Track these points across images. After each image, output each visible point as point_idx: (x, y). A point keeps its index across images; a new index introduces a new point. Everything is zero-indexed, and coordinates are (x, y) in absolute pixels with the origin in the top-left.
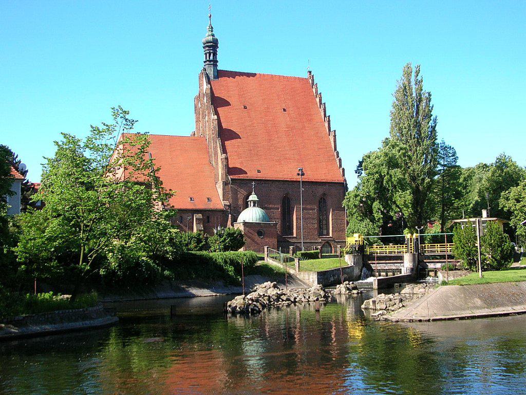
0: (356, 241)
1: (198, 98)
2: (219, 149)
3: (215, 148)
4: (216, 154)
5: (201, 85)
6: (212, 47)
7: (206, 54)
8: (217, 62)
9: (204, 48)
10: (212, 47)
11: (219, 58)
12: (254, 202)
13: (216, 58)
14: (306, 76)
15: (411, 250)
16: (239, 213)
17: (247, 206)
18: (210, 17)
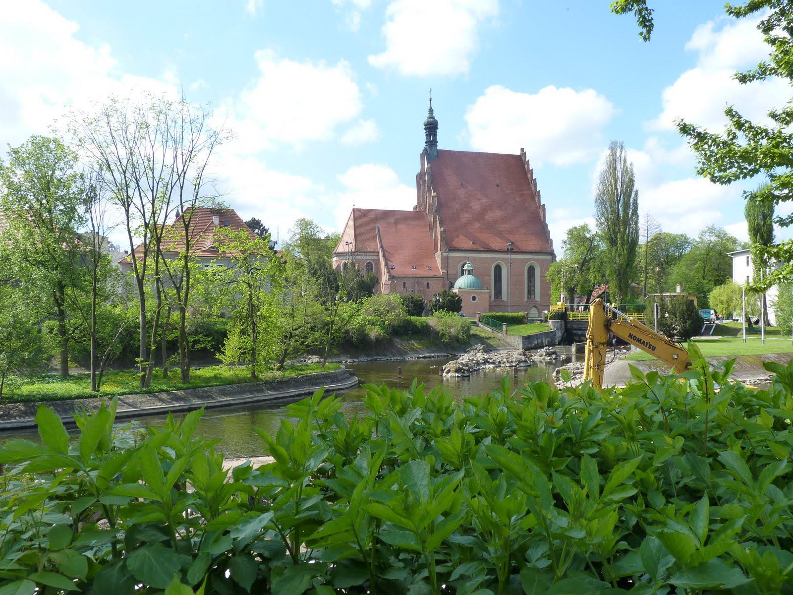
1: (420, 176)
2: (438, 222)
3: (435, 222)
4: (435, 227)
5: (422, 164)
6: (431, 128)
7: (427, 135)
8: (437, 142)
9: (425, 129)
10: (431, 128)
11: (438, 138)
12: (469, 271)
14: (518, 153)
16: (456, 279)
17: (463, 274)
18: (431, 100)
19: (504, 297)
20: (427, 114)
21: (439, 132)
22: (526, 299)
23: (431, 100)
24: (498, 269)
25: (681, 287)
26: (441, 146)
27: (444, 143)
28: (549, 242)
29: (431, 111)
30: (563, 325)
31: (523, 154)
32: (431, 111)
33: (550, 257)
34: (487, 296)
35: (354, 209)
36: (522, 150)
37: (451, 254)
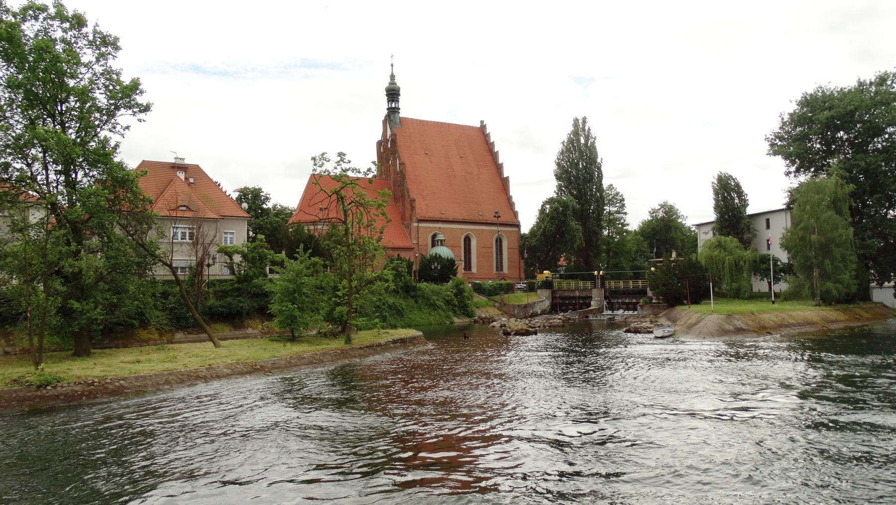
0: (546, 277)
5: (385, 131)
6: (393, 94)
7: (388, 102)
8: (399, 109)
9: (387, 95)
10: (393, 94)
12: (441, 241)
13: (398, 105)
18: (392, 65)
19: (474, 269)
21: (401, 98)
22: (495, 271)
23: (392, 65)
24: (467, 240)
25: (677, 252)
26: (403, 114)
27: (408, 109)
29: (392, 77)
30: (551, 295)
31: (483, 127)
32: (392, 77)
33: (516, 229)
35: (313, 176)
36: (482, 122)
37: (422, 225)
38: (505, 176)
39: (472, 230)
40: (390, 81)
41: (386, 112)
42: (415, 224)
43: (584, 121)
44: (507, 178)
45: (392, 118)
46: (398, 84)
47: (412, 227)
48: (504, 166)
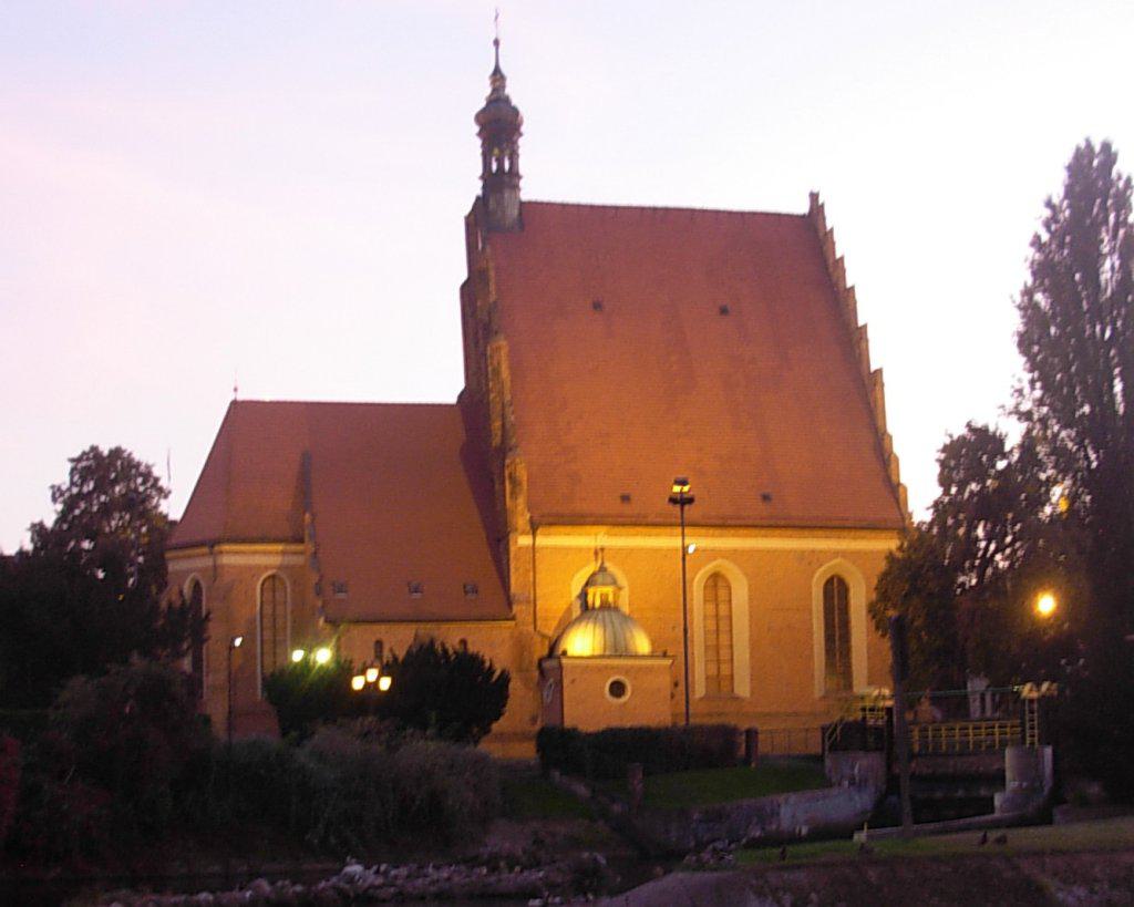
0: (864, 709)
11: (524, 166)
14: (802, 208)
15: (1033, 736)
18: (496, 43)
20: (486, 90)
21: (524, 145)
28: (895, 492)
31: (817, 209)
32: (498, 76)
34: (666, 681)
35: (234, 404)
36: (814, 197)
38: (873, 368)
39: (733, 555)
40: (488, 91)
41: (476, 188)
42: (524, 541)
43: (1109, 156)
44: (879, 372)
45: (492, 204)
46: (515, 102)
47: (513, 549)
48: (871, 334)
